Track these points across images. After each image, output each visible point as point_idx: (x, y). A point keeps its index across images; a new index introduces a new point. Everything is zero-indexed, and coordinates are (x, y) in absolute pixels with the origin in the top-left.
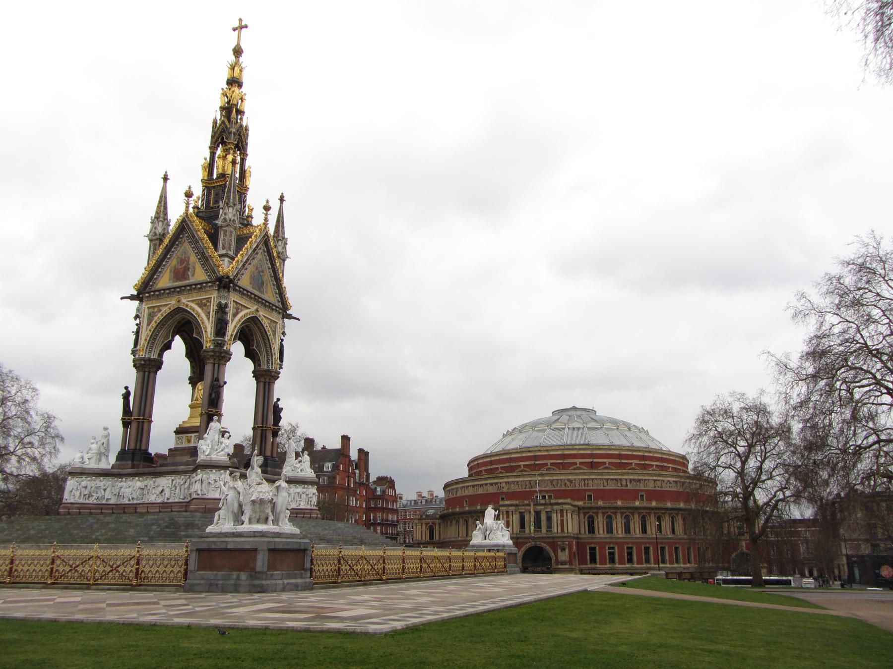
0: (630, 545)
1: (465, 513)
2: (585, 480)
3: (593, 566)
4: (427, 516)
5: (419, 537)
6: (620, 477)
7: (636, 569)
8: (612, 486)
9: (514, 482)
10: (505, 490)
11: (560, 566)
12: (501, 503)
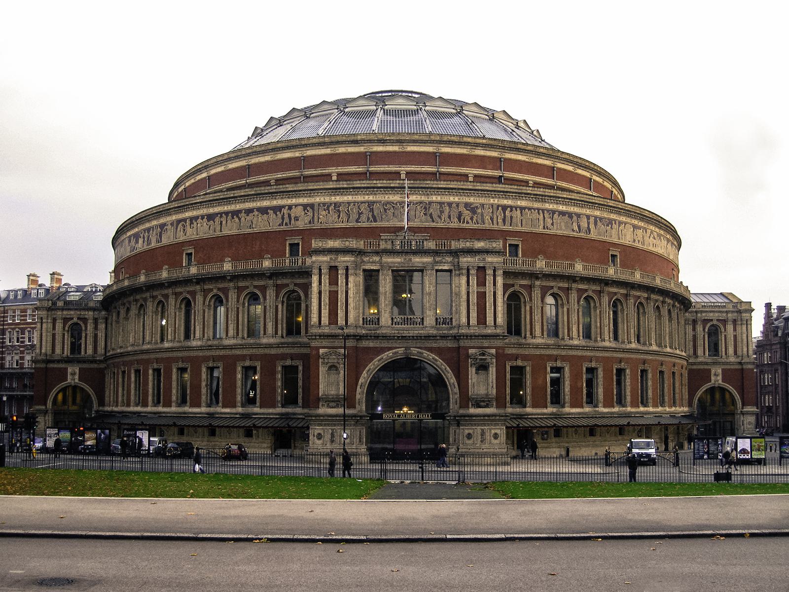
0: (593, 365)
1: (187, 281)
2: (505, 208)
3: (518, 410)
4: (67, 303)
5: (46, 348)
6: (576, 210)
7: (603, 416)
8: (560, 228)
9: (326, 206)
10: (301, 225)
11: (472, 411)
12: (316, 244)
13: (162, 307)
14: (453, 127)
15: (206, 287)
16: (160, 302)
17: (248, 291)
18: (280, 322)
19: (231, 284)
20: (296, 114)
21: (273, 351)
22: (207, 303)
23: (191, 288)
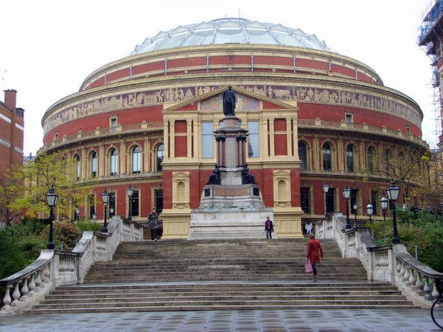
13: (78, 158)
14: (266, 40)
15: (106, 143)
16: (76, 155)
17: (131, 145)
18: (153, 166)
19: (122, 141)
20: (163, 35)
21: (149, 181)
22: (106, 153)
23: (95, 145)
